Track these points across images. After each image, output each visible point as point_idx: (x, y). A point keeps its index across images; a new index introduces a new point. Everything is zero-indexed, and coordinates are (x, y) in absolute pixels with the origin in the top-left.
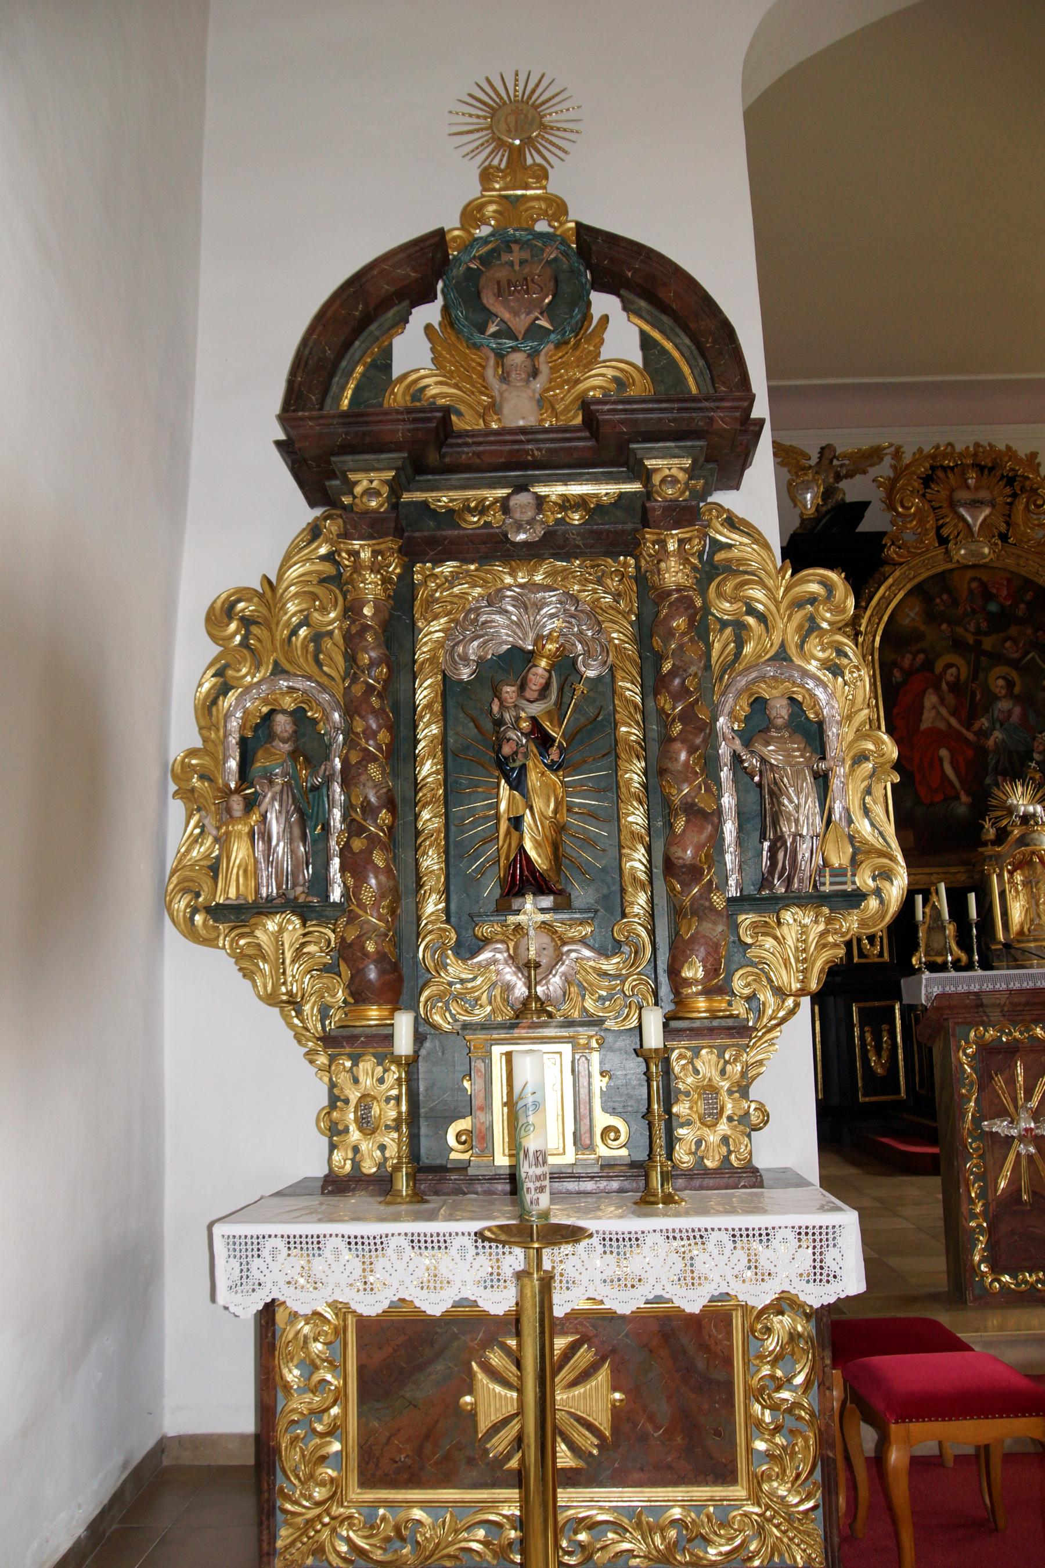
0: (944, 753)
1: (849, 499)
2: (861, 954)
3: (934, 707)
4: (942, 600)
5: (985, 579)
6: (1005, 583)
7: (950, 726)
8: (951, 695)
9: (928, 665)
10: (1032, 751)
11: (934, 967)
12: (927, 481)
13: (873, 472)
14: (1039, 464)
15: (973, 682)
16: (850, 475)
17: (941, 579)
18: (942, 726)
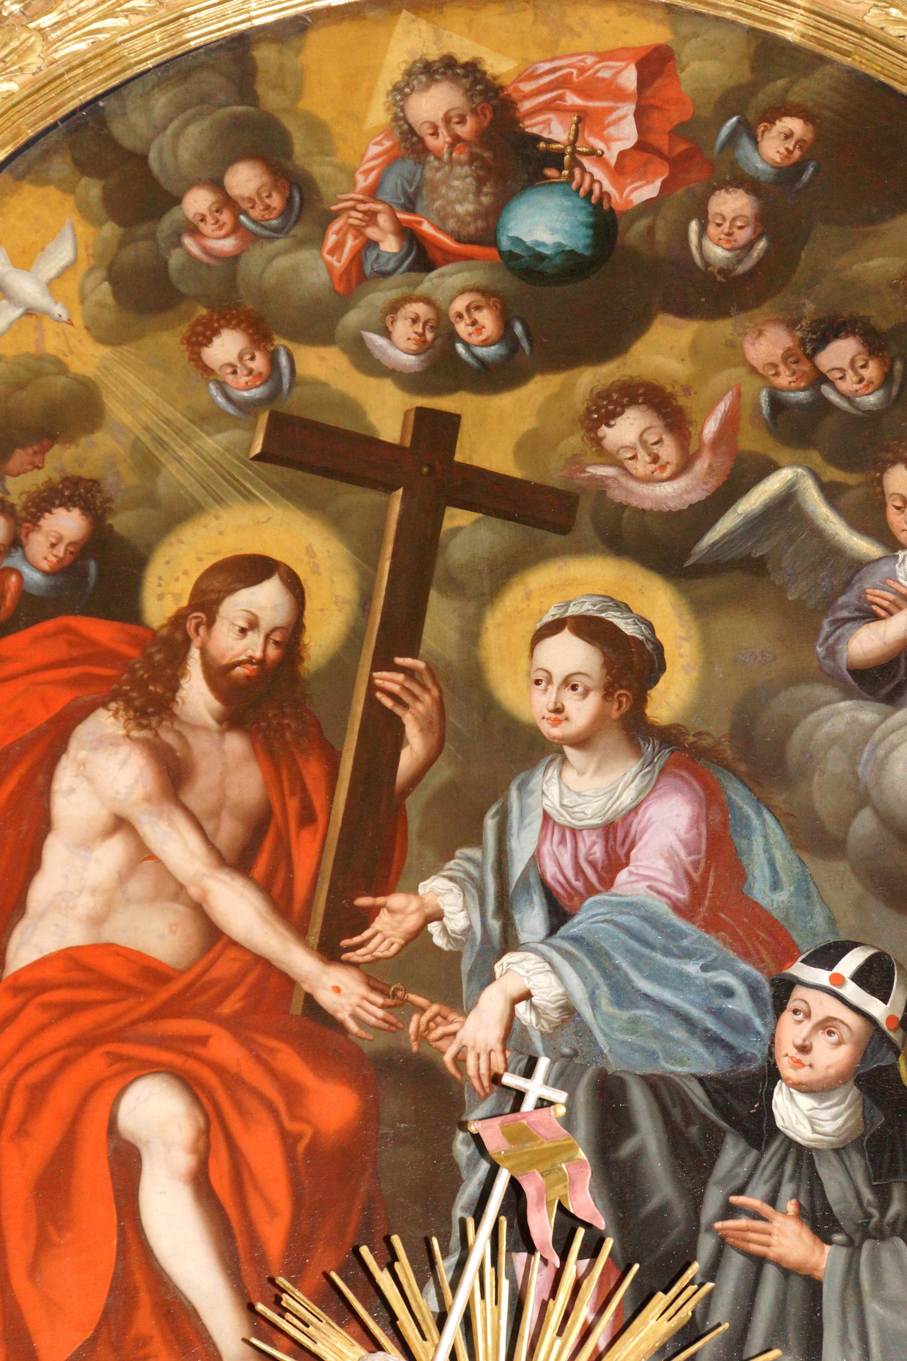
4: (227, 202)
6: (629, 78)
8: (236, 743)
10: (772, 1075)
15: (383, 662)
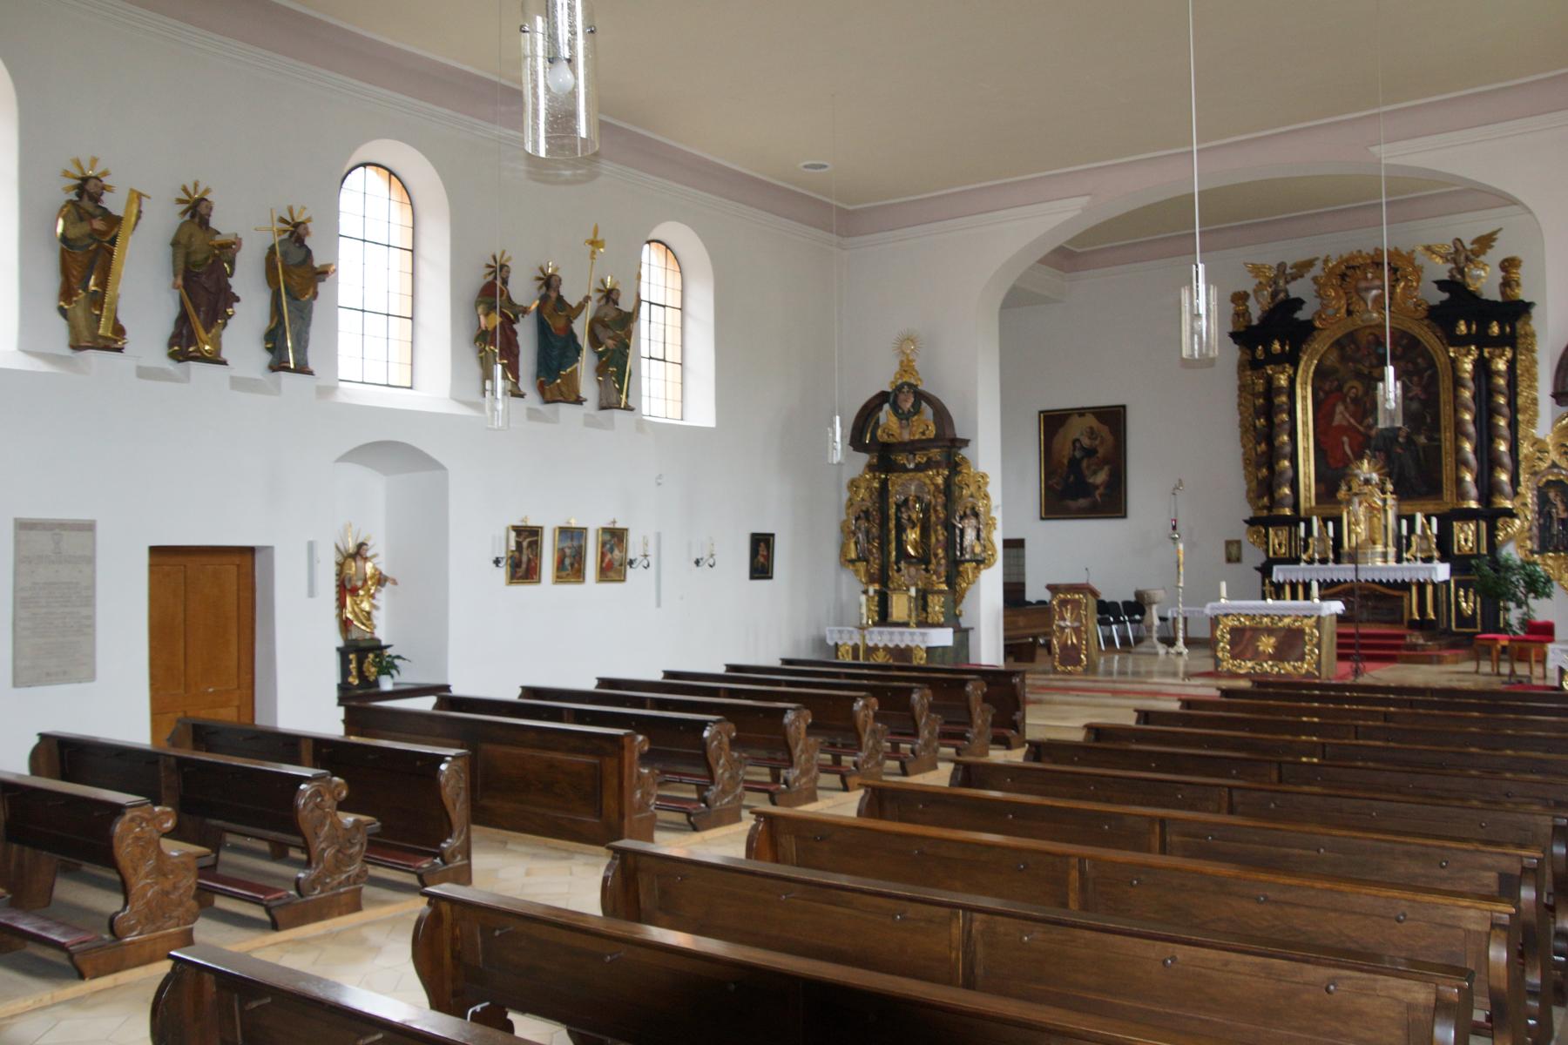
0: (1345, 439)
1: (1292, 295)
2: (1274, 553)
3: (1341, 413)
5: (1377, 333)
7: (1349, 421)
9: (1340, 388)
11: (1311, 561)
12: (1343, 276)
13: (1308, 276)
14: (1414, 259)
16: (1294, 278)
17: (1351, 336)
18: (1345, 423)
